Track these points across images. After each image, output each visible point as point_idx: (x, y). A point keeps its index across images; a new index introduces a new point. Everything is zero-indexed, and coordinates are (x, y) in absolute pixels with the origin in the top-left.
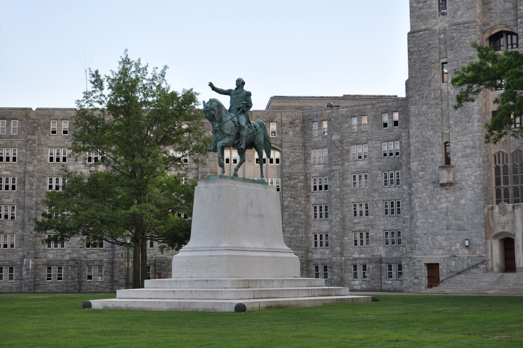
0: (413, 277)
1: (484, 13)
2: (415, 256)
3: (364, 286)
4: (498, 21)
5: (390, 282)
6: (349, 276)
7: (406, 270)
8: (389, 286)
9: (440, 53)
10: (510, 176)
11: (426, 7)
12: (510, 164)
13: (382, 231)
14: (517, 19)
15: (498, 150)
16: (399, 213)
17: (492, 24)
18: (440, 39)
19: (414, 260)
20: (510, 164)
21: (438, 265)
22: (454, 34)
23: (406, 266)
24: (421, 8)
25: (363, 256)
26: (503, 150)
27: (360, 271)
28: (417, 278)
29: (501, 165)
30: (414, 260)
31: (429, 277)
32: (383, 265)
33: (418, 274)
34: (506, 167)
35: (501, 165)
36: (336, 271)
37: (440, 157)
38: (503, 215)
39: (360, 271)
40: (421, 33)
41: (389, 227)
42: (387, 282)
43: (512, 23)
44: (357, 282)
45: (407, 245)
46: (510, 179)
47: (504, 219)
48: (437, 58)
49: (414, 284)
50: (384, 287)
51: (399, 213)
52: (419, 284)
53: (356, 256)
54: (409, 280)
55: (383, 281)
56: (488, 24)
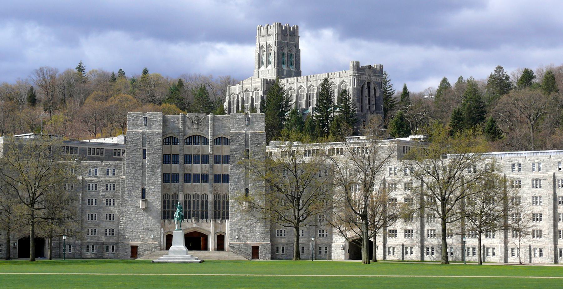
1: (163, 127)
3: (93, 256)
4: (170, 132)
6: (85, 251)
10: (171, 205)
12: (171, 200)
14: (179, 133)
15: (165, 192)
17: (167, 133)
20: (171, 200)
24: (134, 120)
25: (92, 241)
27: (90, 248)
31: (131, 252)
33: (127, 251)
34: (169, 201)
36: (78, 248)
37: (140, 195)
39: (90, 248)
43: (177, 134)
44: (89, 254)
47: (170, 226)
50: (104, 257)
52: (127, 255)
53: (89, 240)
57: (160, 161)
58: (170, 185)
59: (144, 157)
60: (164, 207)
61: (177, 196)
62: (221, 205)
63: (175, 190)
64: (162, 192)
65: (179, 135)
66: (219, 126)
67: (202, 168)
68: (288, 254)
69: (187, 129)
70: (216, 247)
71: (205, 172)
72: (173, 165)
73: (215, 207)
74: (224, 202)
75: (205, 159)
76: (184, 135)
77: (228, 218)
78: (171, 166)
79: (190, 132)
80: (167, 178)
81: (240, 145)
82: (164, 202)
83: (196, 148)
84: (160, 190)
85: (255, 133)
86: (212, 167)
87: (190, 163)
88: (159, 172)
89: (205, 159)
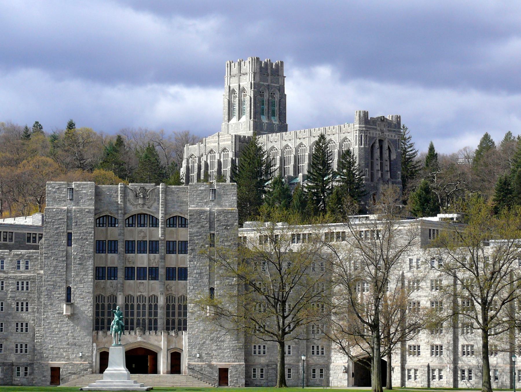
0: (42, 376)
2: (43, 362)
5: (19, 379)
7: (37, 371)
8: (17, 382)
9: (67, 226)
11: (58, 192)
12: (106, 304)
13: (13, 343)
14: (118, 210)
16: (27, 331)
17: (101, 210)
18: (67, 217)
19: (43, 365)
20: (106, 304)
21: (59, 368)
22: (78, 215)
23: (36, 369)
24: (55, 192)
26: (102, 294)
28: (45, 377)
29: (100, 304)
30: (43, 365)
31: (52, 376)
32: (14, 367)
33: (45, 374)
34: (103, 305)
35: (100, 304)
37: (64, 296)
38: (105, 338)
40: (54, 210)
41: (18, 341)
42: (16, 379)
43: (115, 212)
45: (38, 354)
46: (106, 314)
47: (105, 340)
48: (65, 229)
49: (42, 381)
50: (14, 382)
51: (27, 331)
52: (45, 381)
54: (39, 378)
55: (13, 378)
56: (99, 210)
57: (91, 250)
58: (106, 283)
59: (69, 244)
60: (97, 314)
61: (115, 299)
62: (177, 311)
63: (112, 290)
64: (94, 292)
65: (118, 214)
66: (173, 200)
67: (149, 260)
68: (270, 379)
69: (128, 204)
70: (169, 369)
71: (154, 265)
72: (110, 255)
73: (168, 314)
74: (180, 306)
75: (153, 247)
76: (125, 214)
77: (185, 329)
78: (106, 257)
79: (133, 210)
80: (102, 273)
81: (202, 227)
82: (97, 307)
83: (141, 231)
84: (91, 290)
85: (223, 211)
86: (163, 258)
87: (133, 252)
88: (90, 264)
89: (153, 247)
